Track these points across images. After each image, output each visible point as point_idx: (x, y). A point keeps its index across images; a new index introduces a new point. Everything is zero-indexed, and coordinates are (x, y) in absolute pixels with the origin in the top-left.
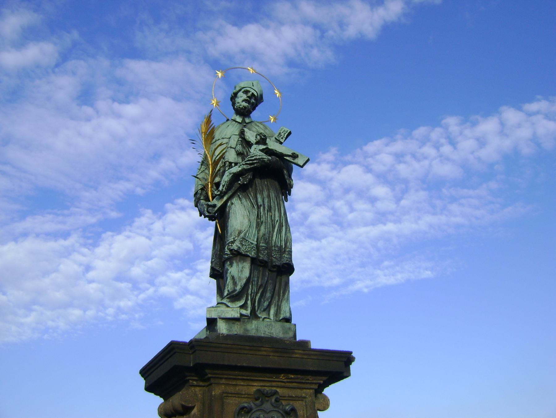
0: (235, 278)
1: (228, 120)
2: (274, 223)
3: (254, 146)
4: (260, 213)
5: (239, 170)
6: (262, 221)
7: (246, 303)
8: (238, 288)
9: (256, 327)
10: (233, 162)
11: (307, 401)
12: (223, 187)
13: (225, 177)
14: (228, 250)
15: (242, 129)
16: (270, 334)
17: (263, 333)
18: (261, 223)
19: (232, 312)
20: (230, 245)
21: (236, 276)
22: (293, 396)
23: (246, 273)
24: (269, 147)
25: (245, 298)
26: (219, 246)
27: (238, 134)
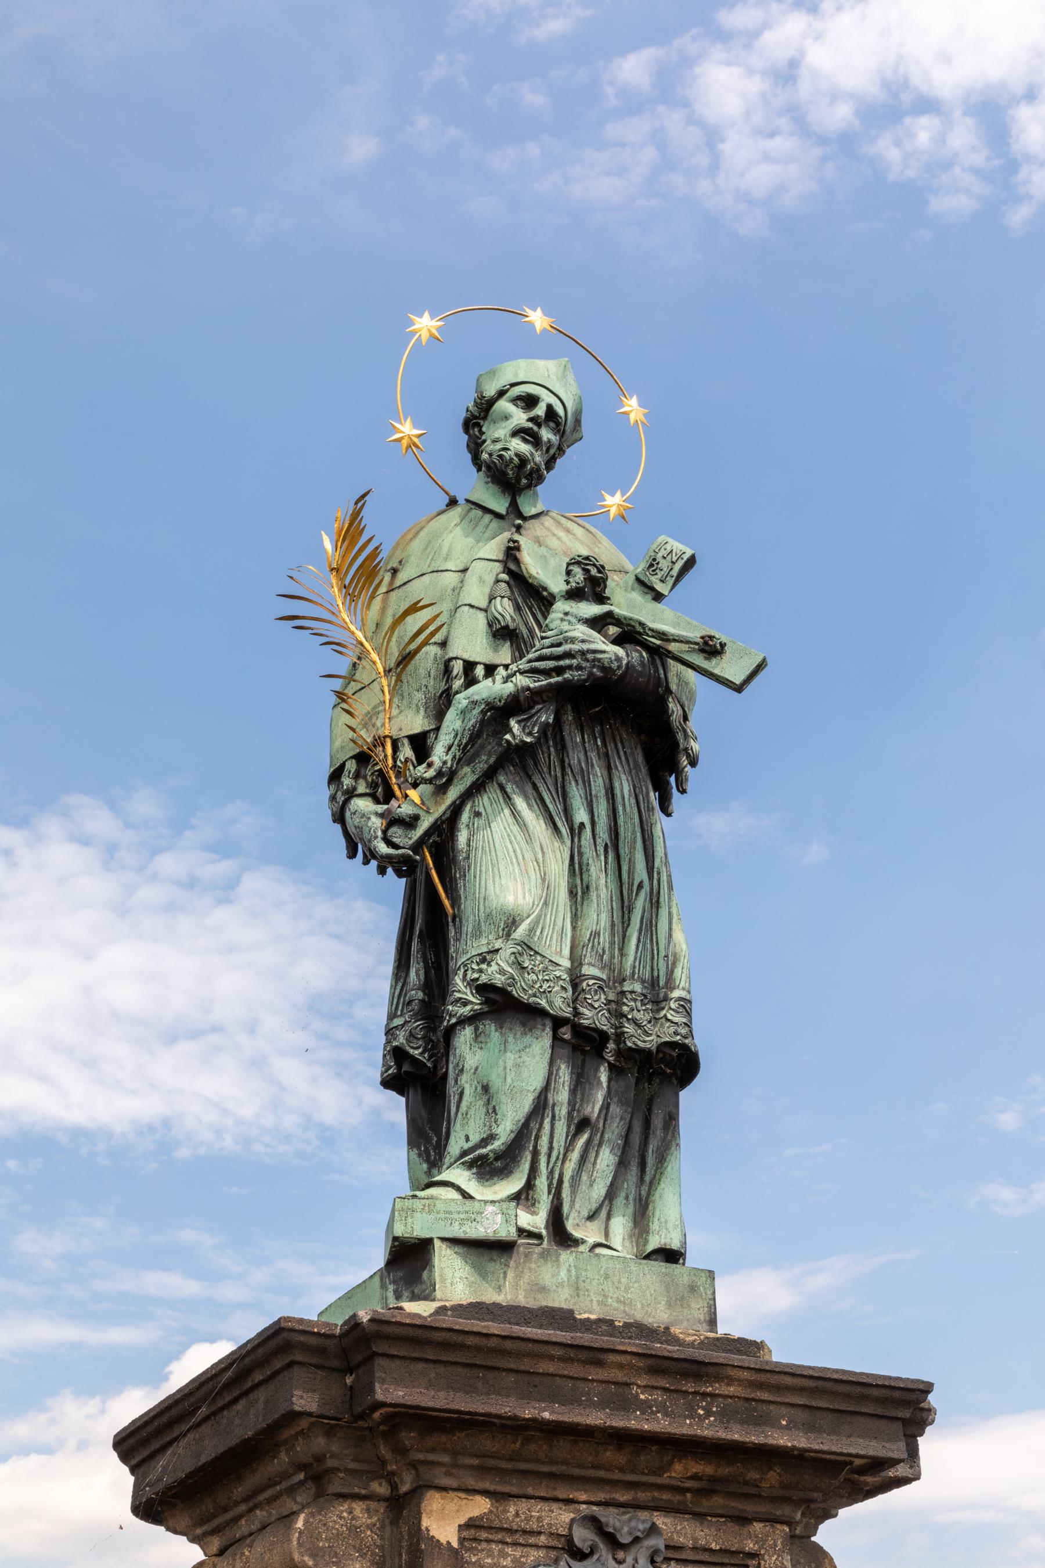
1: (453, 502)
2: (630, 890)
3: (561, 606)
4: (581, 854)
6: (588, 887)
7: (529, 1185)
8: (505, 1130)
10: (478, 660)
14: (466, 987)
17: (598, 1301)
18: (583, 893)
20: (475, 967)
21: (496, 1082)
22: (713, 1546)
24: (617, 610)
25: (525, 1166)
26: (422, 973)
27: (494, 558)
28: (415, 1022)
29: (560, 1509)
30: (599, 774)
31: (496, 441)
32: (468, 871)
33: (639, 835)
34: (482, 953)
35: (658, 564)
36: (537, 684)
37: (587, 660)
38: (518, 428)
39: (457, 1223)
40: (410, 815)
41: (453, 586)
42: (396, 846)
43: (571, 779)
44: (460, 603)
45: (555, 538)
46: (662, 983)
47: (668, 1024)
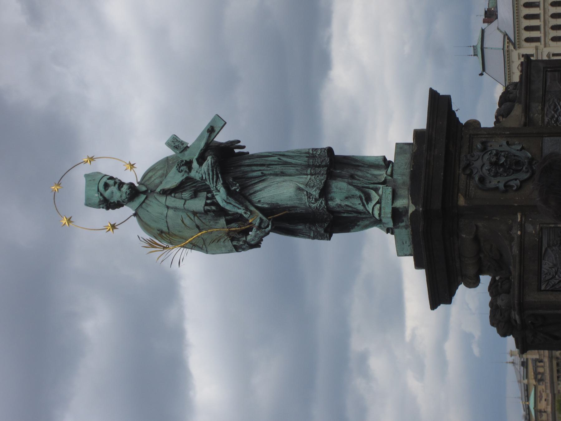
0: (347, 196)
2: (280, 162)
3: (193, 174)
5: (224, 190)
6: (282, 172)
7: (372, 189)
8: (358, 193)
10: (204, 202)
12: (241, 209)
13: (228, 207)
14: (317, 203)
15: (160, 192)
20: (311, 199)
24: (196, 157)
25: (367, 189)
27: (165, 198)
28: (316, 225)
30: (243, 168)
31: (121, 196)
32: (278, 204)
33: (263, 158)
35: (176, 146)
36: (221, 181)
37: (214, 166)
43: (246, 176)
44: (183, 208)
46: (308, 155)
47: (321, 154)
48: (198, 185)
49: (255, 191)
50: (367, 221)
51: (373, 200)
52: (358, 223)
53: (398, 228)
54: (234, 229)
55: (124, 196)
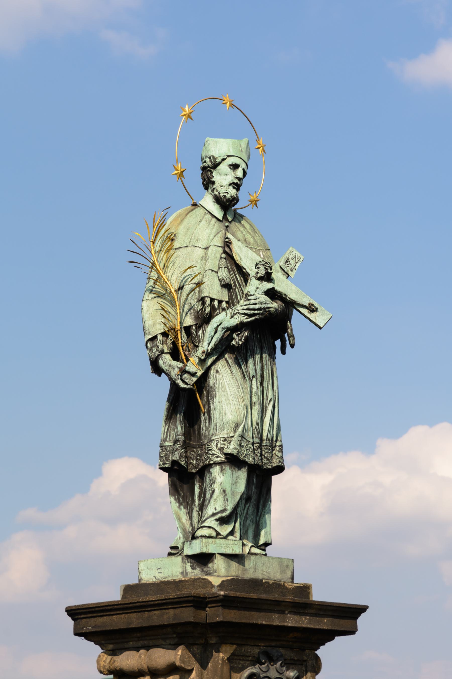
0: (227, 492)
5: (235, 324)
6: (255, 403)
8: (230, 508)
9: (254, 565)
10: (215, 298)
11: (308, 665)
14: (218, 450)
15: (228, 238)
16: (267, 575)
17: (261, 573)
19: (232, 546)
20: (222, 442)
21: (228, 490)
22: (295, 659)
23: (241, 487)
27: (220, 245)
28: (181, 450)
29: (256, 648)
32: (215, 398)
34: (225, 437)
35: (289, 261)
38: (232, 182)
39: (223, 548)
40: (194, 372)
41: (202, 256)
42: (187, 384)
44: (208, 269)
45: (240, 233)
46: (274, 440)
48: (237, 290)
49: (230, 367)
50: (186, 519)
51: (220, 527)
52: (182, 507)
53: (183, 561)
54: (179, 337)
55: (222, 190)
